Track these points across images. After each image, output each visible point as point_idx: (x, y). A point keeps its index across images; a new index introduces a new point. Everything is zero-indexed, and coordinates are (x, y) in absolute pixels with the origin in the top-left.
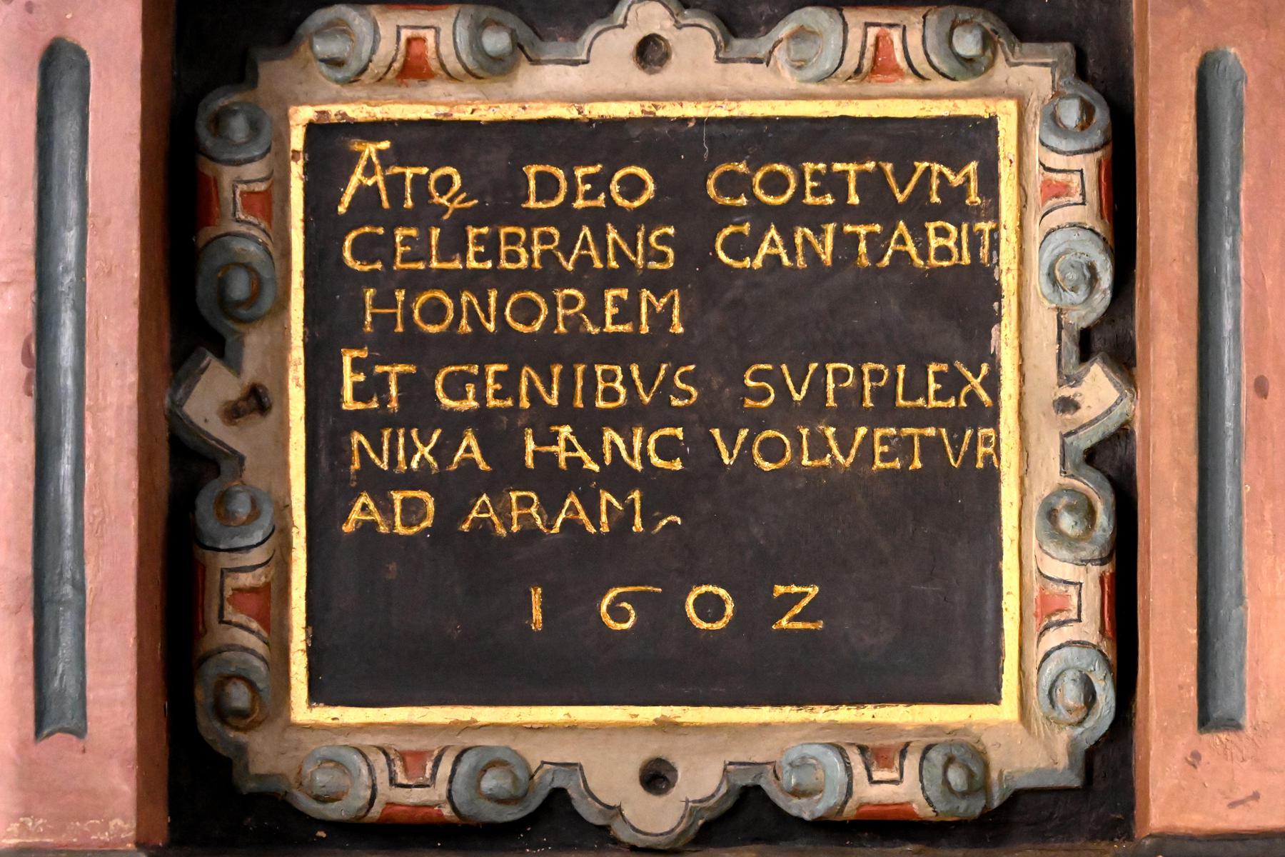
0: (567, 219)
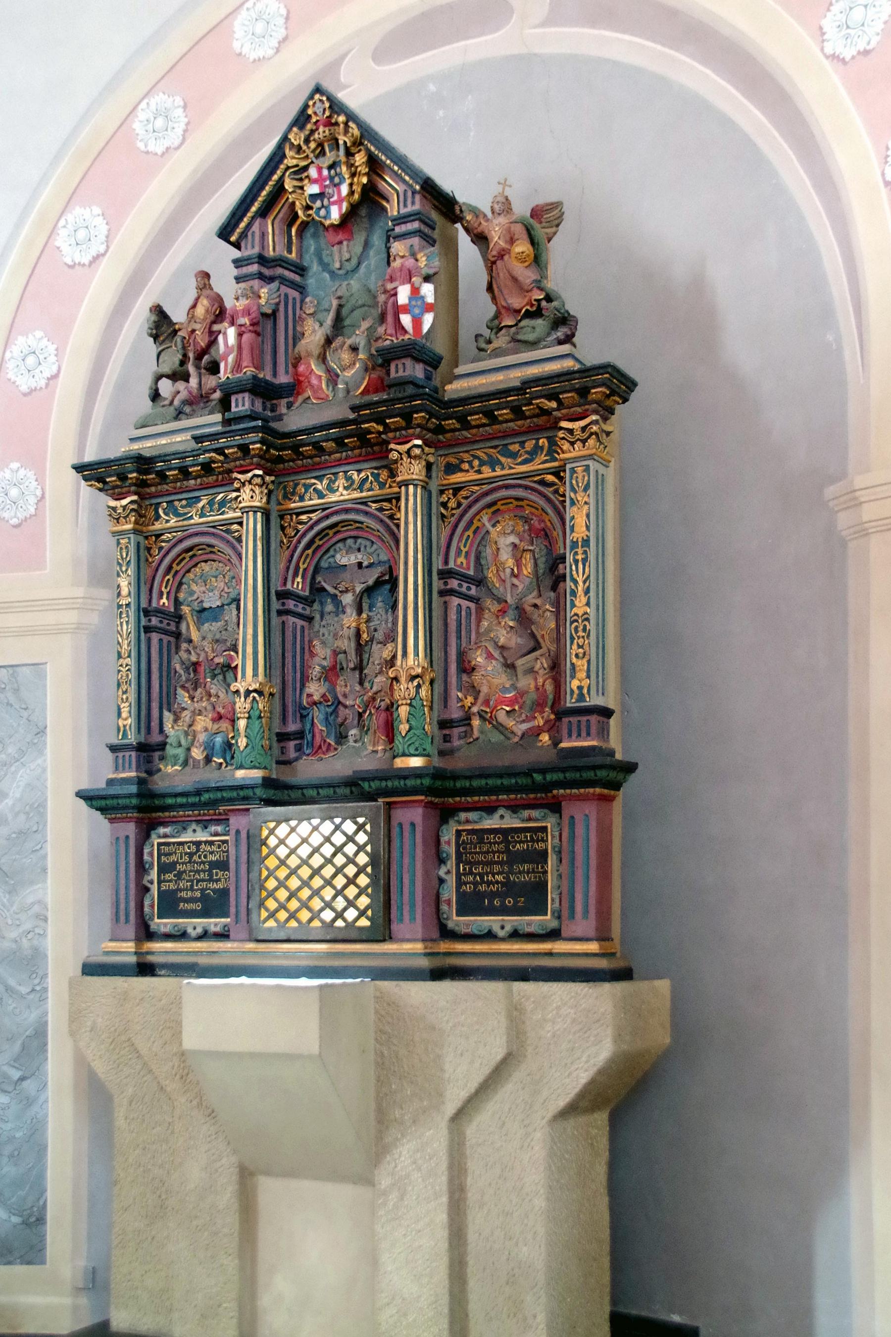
0: (490, 843)
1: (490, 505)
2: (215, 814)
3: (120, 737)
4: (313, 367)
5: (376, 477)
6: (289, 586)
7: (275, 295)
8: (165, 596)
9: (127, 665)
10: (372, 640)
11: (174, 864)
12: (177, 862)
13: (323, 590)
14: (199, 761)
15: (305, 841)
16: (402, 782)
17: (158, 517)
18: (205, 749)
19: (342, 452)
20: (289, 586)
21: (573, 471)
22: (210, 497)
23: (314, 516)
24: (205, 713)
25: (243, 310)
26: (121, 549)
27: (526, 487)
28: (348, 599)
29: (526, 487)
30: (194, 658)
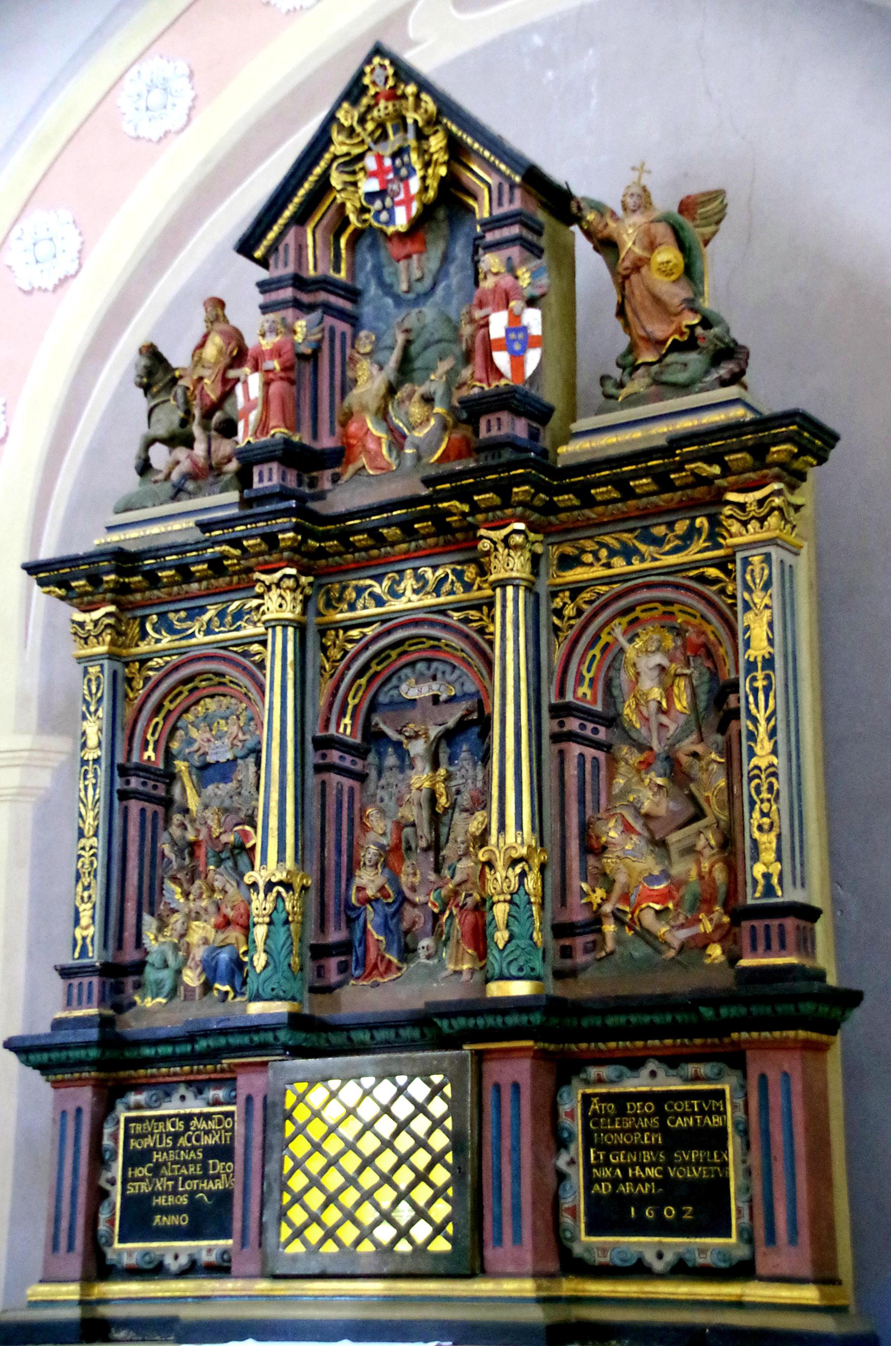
0: (636, 1115)
1: (624, 612)
2: (215, 1071)
3: (77, 955)
4: (370, 425)
5: (459, 575)
6: (332, 731)
7: (316, 329)
8: (151, 747)
9: (91, 848)
10: (453, 806)
11: (149, 1151)
12: (155, 1149)
13: (383, 735)
14: (193, 990)
15: (351, 1112)
16: (499, 1020)
17: (144, 635)
18: (204, 970)
19: (410, 542)
20: (332, 731)
21: (746, 562)
22: (220, 607)
23: (370, 631)
24: (205, 917)
25: (271, 350)
26: (90, 680)
27: (677, 586)
28: (417, 748)
29: (677, 586)
30: (191, 836)
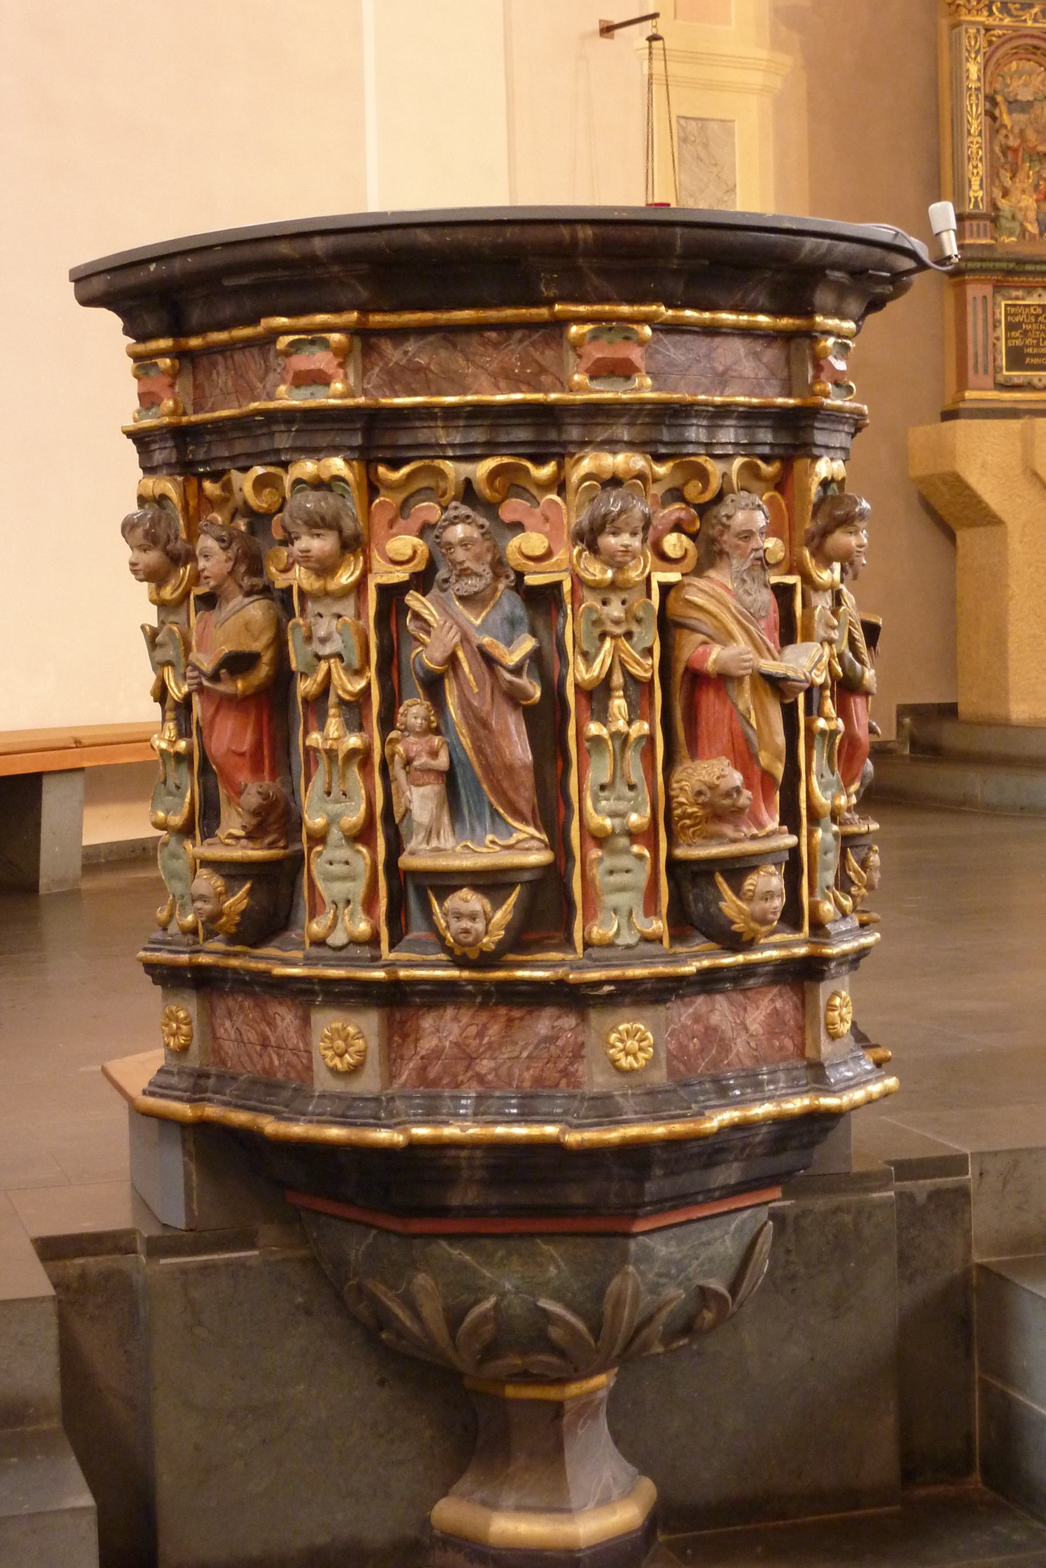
17: (991, 13)
26: (969, 37)
